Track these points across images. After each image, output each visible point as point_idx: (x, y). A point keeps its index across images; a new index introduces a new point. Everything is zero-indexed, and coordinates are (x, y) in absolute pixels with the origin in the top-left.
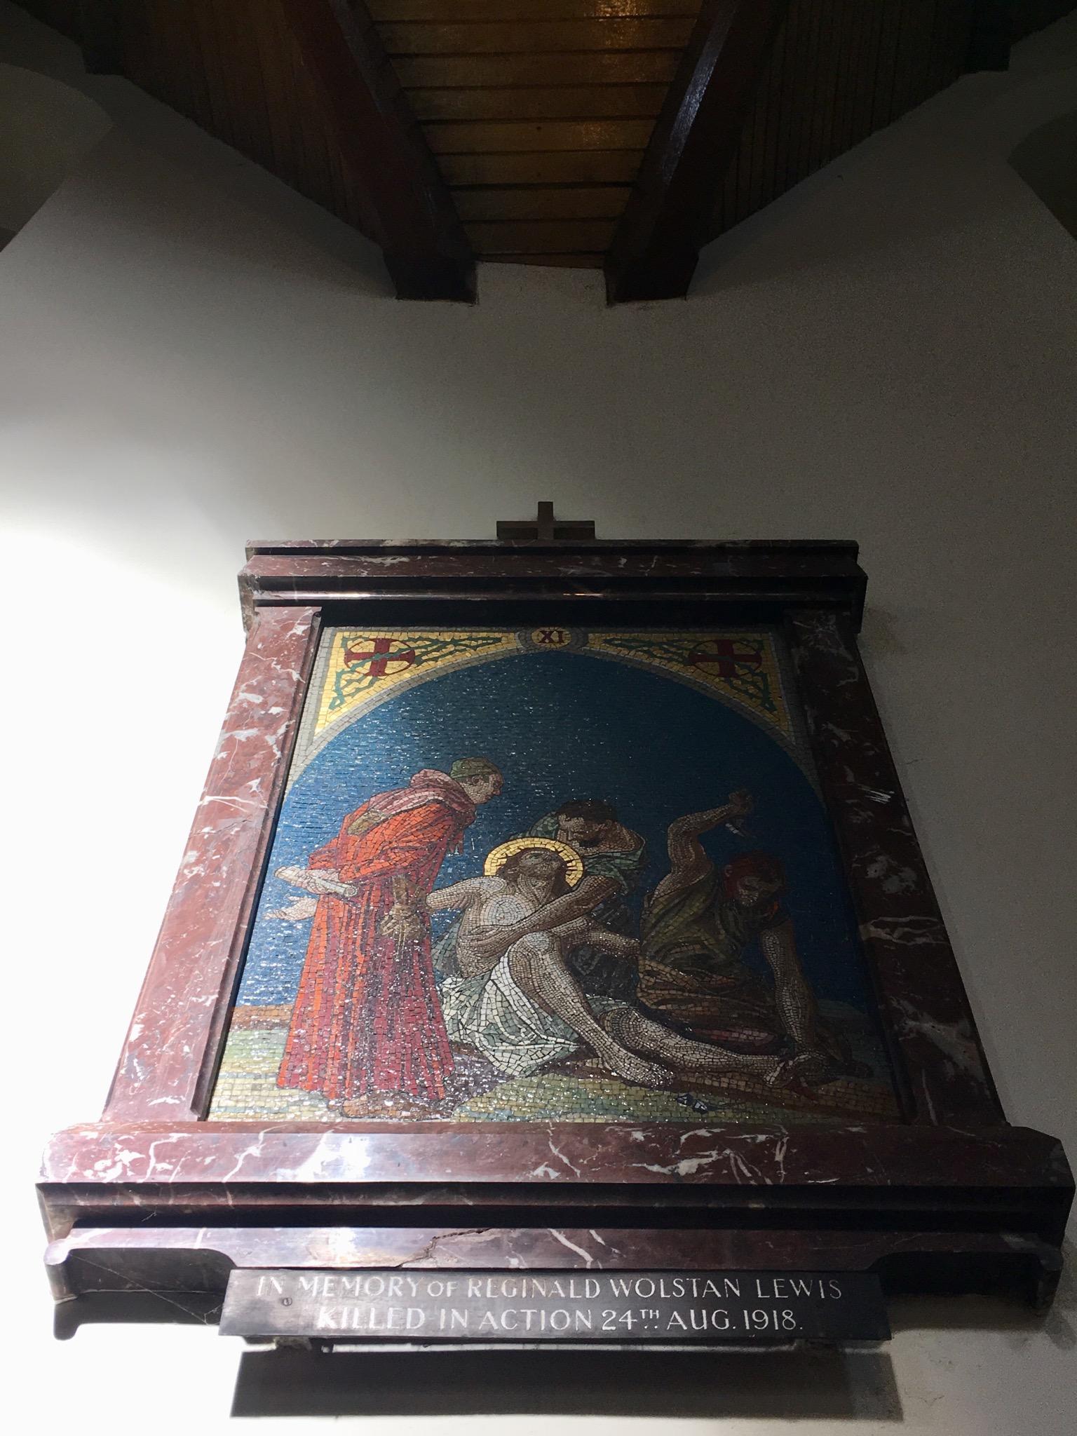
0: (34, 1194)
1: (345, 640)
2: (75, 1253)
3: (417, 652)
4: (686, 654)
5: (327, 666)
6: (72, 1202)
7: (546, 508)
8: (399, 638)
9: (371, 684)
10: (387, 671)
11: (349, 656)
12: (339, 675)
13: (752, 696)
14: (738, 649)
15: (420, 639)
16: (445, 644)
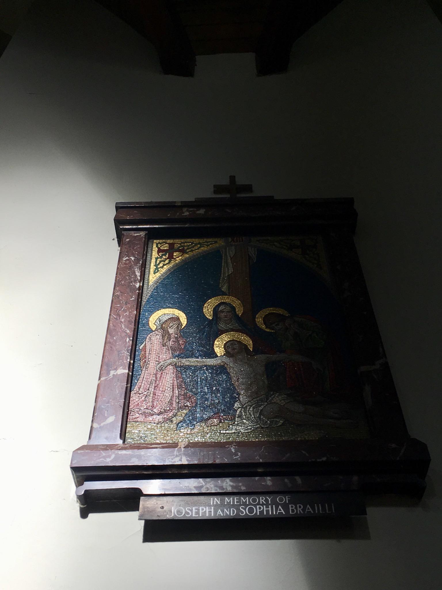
0: (69, 472)
2: (86, 491)
3: (186, 248)
5: (151, 256)
6: (82, 474)
7: (232, 178)
8: (178, 243)
11: (159, 251)
12: (157, 259)
16: (196, 245)
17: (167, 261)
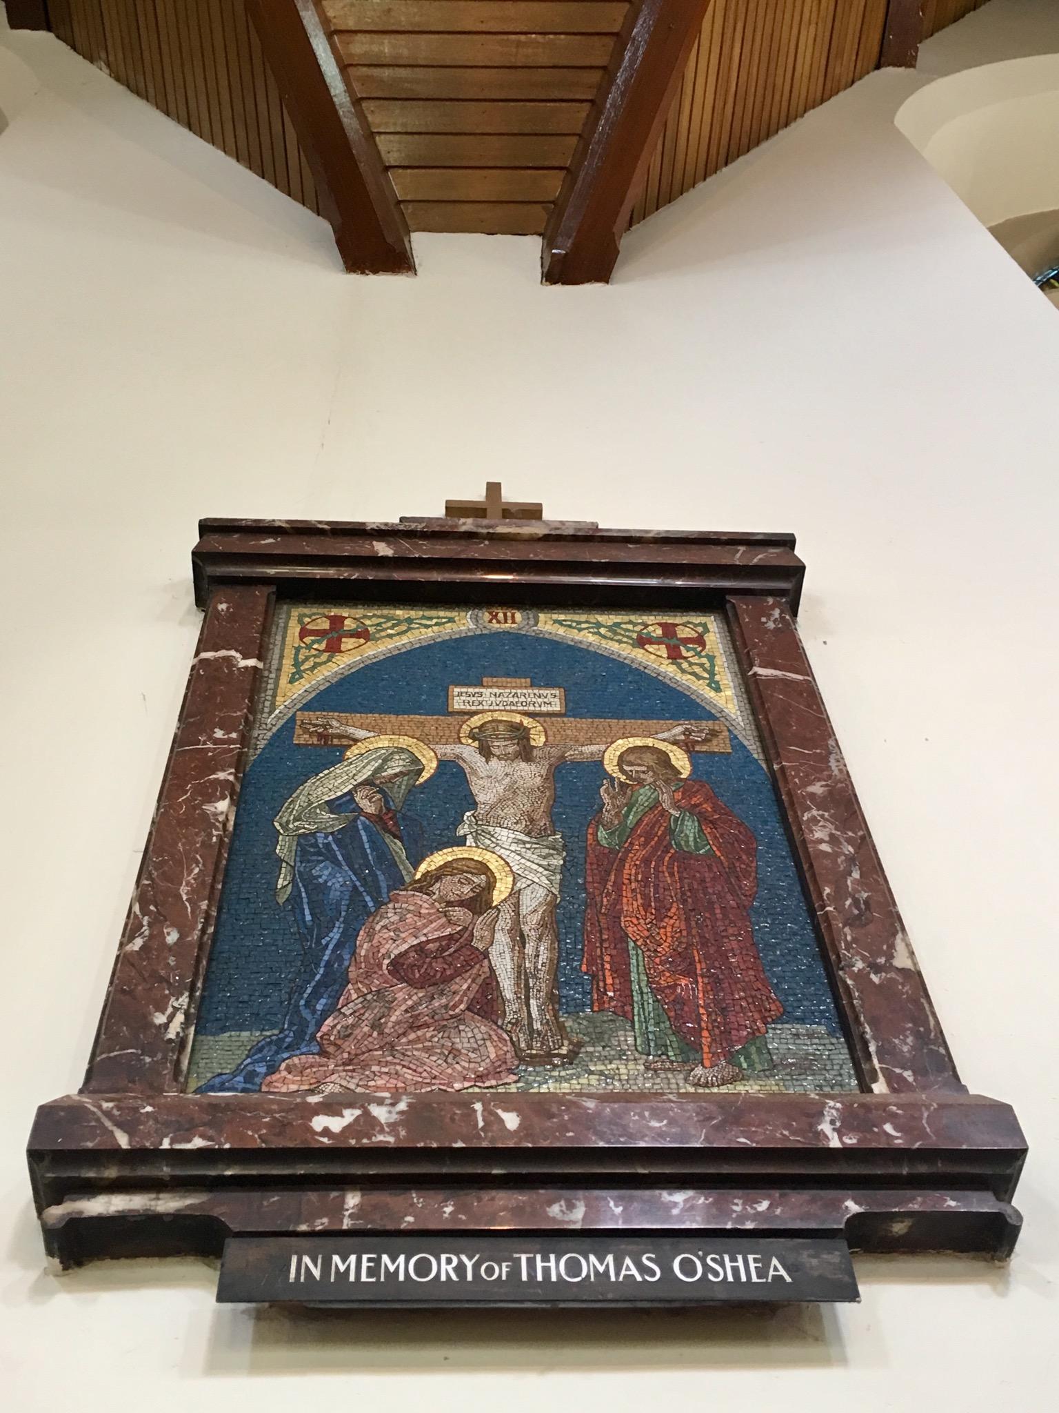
1: (301, 617)
3: (372, 630)
4: (635, 636)
8: (351, 616)
9: (329, 660)
10: (343, 647)
11: (304, 633)
12: (298, 650)
13: (698, 677)
14: (684, 633)
15: (374, 616)
16: (400, 622)
17: (325, 657)
